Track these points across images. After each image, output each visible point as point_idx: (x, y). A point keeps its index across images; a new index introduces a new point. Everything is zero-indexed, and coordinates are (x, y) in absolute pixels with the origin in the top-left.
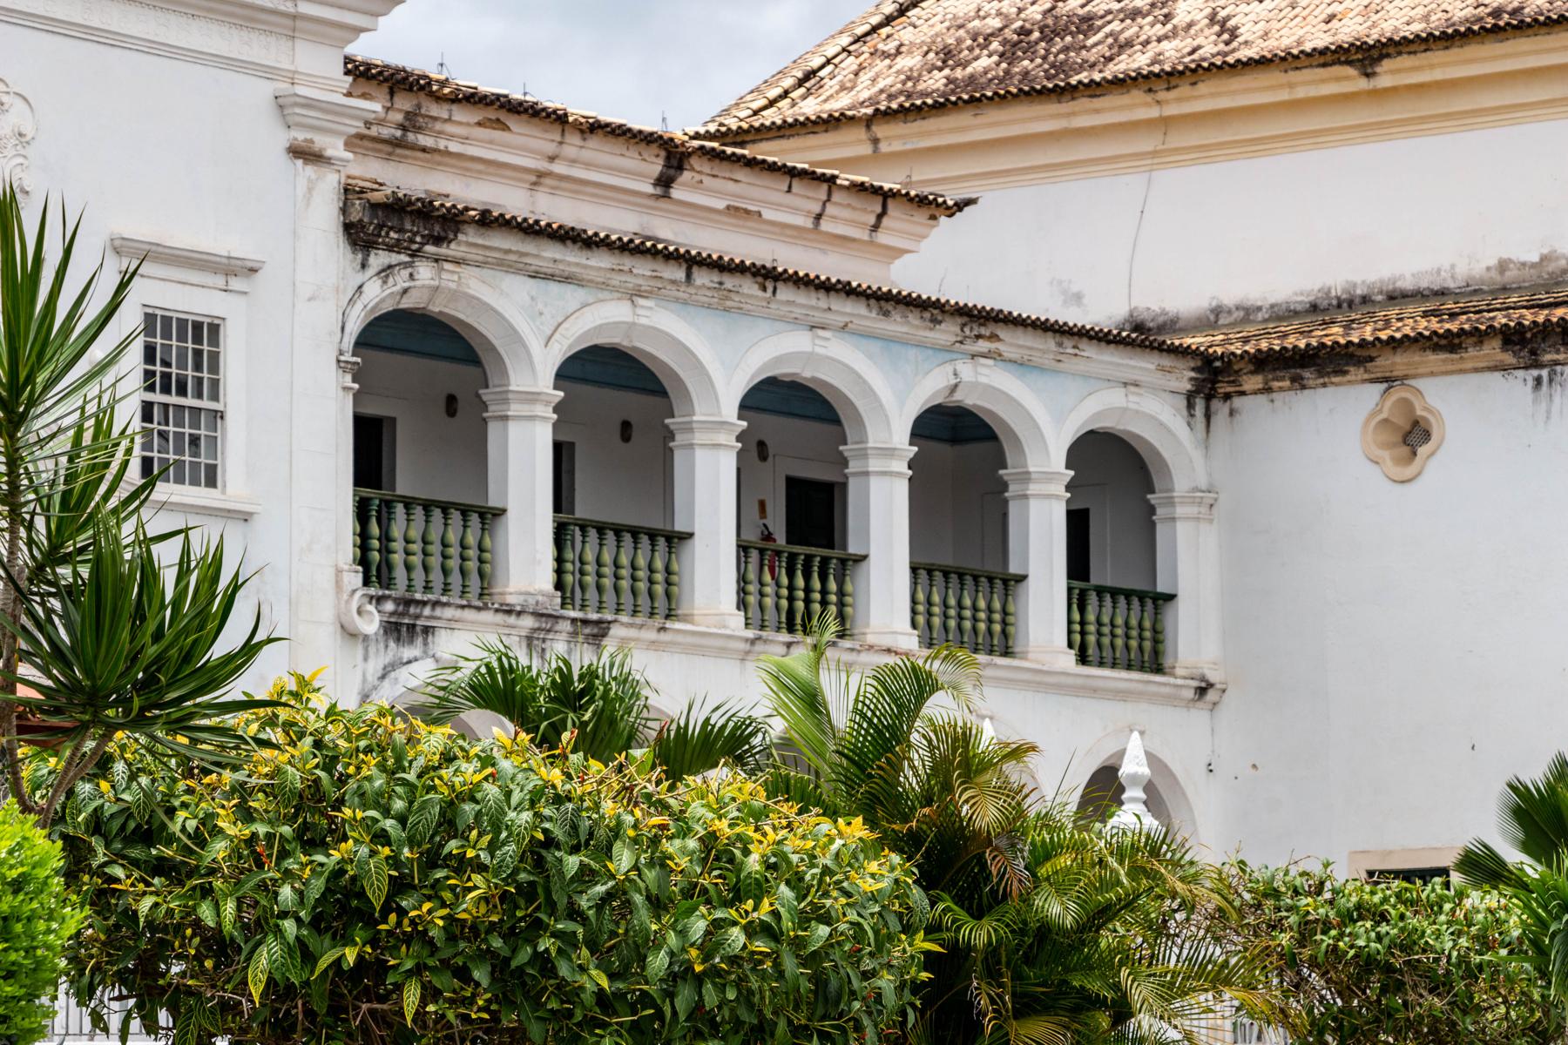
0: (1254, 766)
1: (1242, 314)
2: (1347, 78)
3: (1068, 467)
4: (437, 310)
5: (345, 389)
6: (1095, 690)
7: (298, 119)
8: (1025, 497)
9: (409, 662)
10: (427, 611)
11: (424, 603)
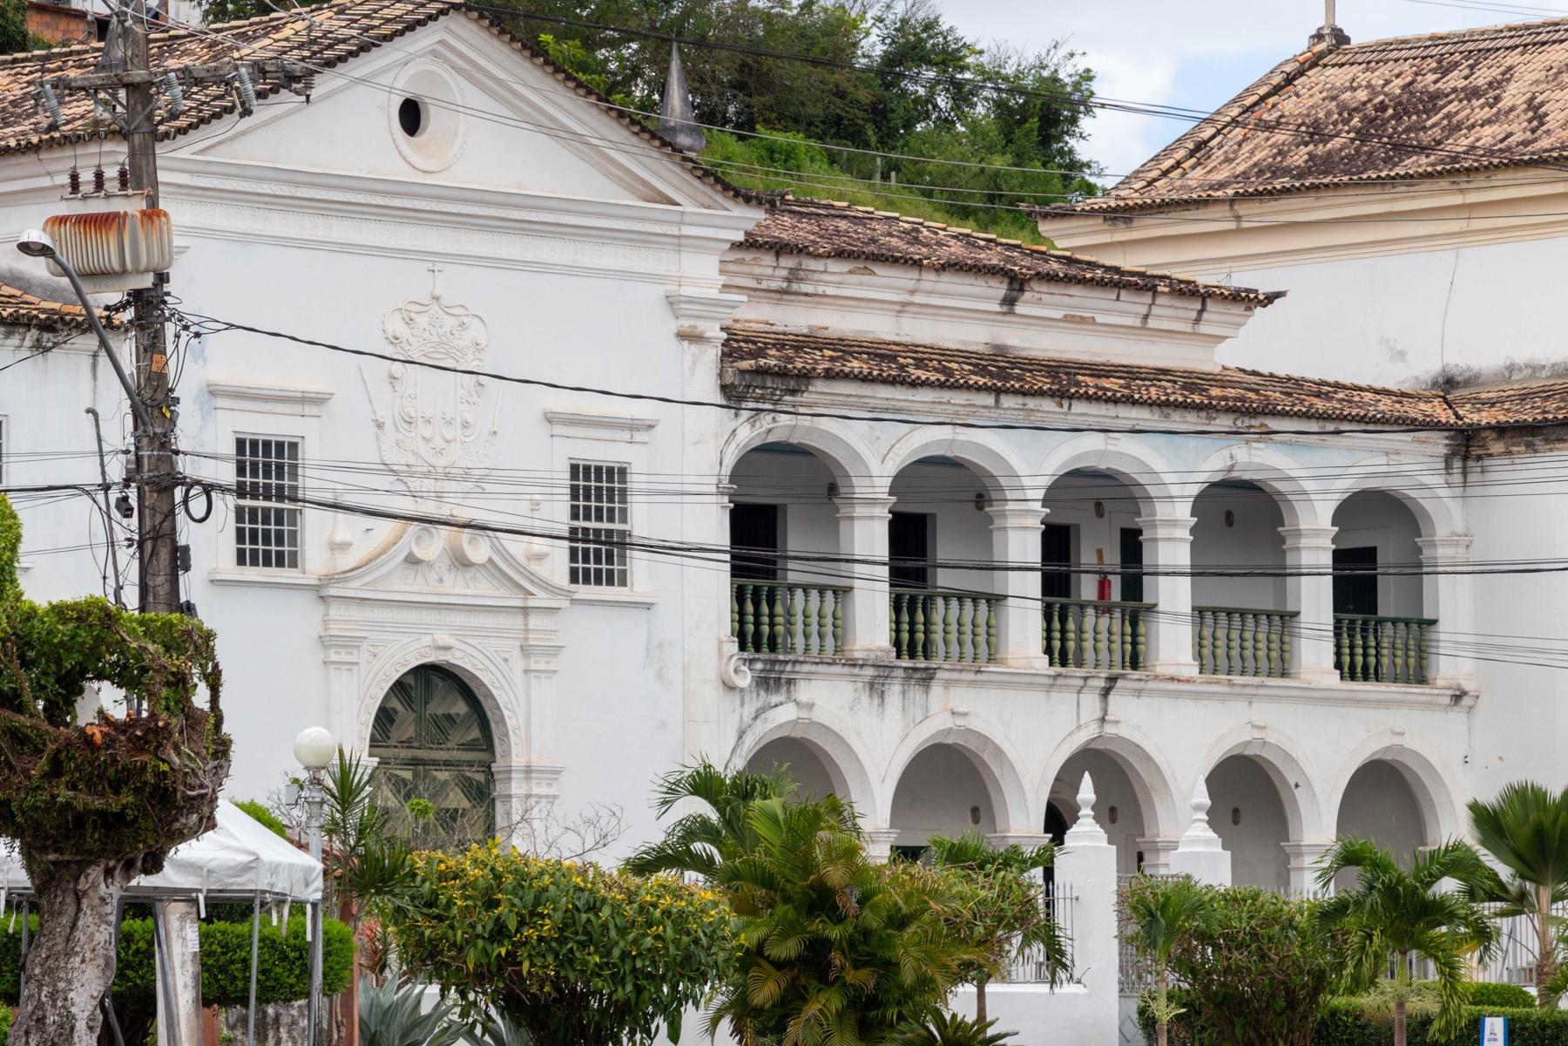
0: (1500, 758)
1: (1530, 371)
3: (1333, 525)
4: (795, 442)
7: (684, 312)
8: (1298, 549)
9: (776, 706)
10: (789, 667)
11: (787, 662)
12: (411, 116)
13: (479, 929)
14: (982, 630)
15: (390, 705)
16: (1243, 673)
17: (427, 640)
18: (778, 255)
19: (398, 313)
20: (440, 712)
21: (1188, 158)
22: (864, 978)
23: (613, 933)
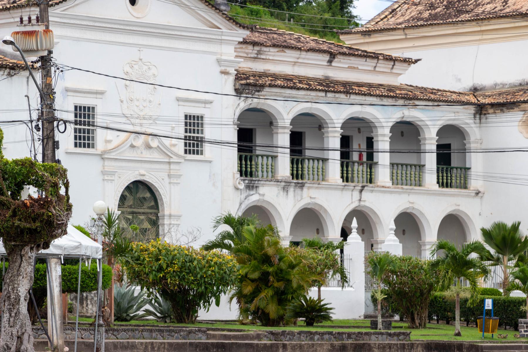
0: (491, 214)
1: (502, 86)
5: (235, 129)
6: (445, 194)
8: (425, 144)
9: (252, 195)
10: (256, 182)
11: (256, 181)
13: (154, 268)
14: (320, 170)
16: (406, 185)
17: (137, 173)
18: (254, 46)
19: (128, 64)
20: (141, 196)
21: (389, 15)
22: (280, 285)
23: (198, 270)
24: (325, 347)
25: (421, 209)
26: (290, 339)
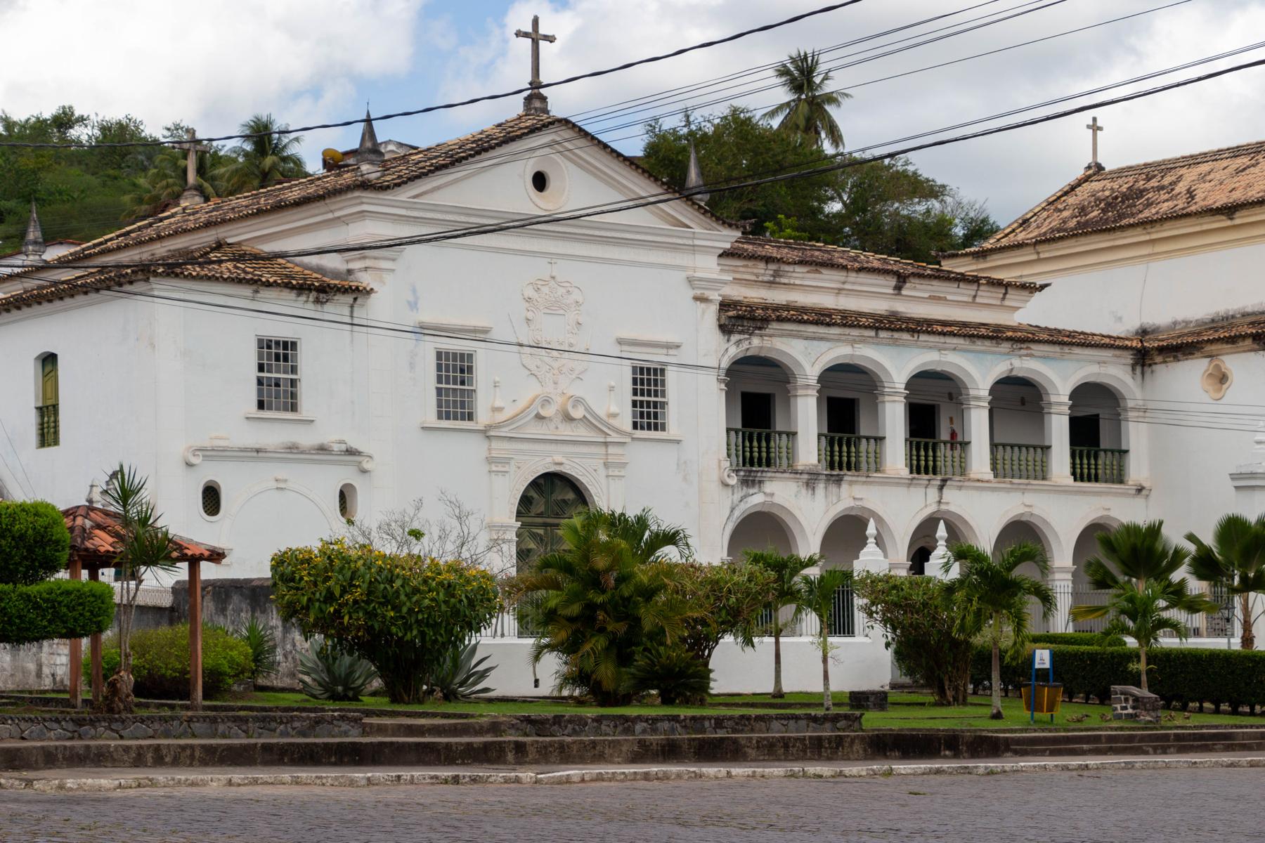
2: (1222, 220)
10: (759, 474)
12: (540, 181)
13: (318, 595)
14: (872, 455)
15: (529, 494)
16: (1020, 478)
17: (549, 460)
18: (767, 262)
19: (531, 287)
21: (1018, 228)
22: (621, 628)
23: (403, 597)
24: (624, 749)
25: (1044, 516)
26: (575, 733)
